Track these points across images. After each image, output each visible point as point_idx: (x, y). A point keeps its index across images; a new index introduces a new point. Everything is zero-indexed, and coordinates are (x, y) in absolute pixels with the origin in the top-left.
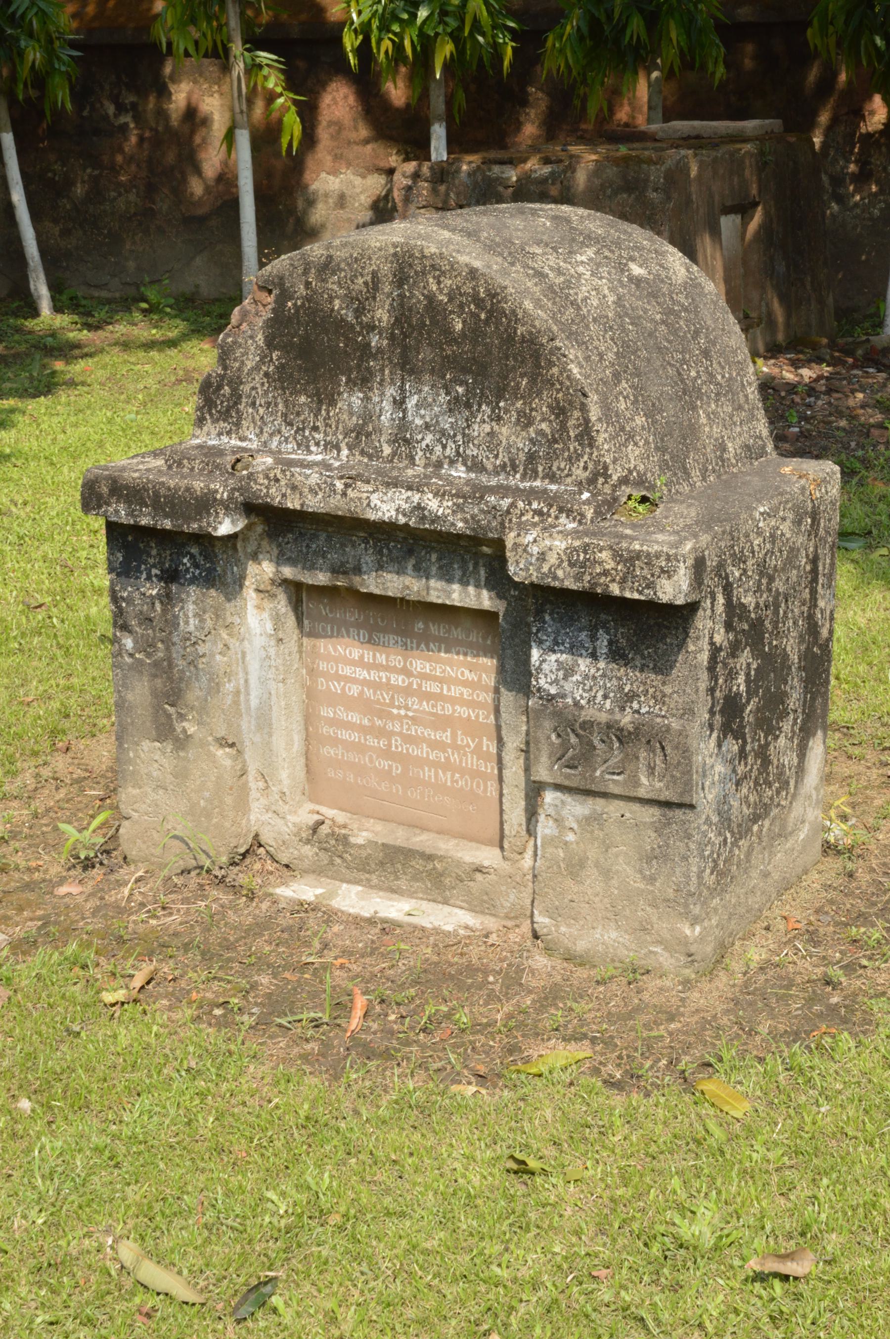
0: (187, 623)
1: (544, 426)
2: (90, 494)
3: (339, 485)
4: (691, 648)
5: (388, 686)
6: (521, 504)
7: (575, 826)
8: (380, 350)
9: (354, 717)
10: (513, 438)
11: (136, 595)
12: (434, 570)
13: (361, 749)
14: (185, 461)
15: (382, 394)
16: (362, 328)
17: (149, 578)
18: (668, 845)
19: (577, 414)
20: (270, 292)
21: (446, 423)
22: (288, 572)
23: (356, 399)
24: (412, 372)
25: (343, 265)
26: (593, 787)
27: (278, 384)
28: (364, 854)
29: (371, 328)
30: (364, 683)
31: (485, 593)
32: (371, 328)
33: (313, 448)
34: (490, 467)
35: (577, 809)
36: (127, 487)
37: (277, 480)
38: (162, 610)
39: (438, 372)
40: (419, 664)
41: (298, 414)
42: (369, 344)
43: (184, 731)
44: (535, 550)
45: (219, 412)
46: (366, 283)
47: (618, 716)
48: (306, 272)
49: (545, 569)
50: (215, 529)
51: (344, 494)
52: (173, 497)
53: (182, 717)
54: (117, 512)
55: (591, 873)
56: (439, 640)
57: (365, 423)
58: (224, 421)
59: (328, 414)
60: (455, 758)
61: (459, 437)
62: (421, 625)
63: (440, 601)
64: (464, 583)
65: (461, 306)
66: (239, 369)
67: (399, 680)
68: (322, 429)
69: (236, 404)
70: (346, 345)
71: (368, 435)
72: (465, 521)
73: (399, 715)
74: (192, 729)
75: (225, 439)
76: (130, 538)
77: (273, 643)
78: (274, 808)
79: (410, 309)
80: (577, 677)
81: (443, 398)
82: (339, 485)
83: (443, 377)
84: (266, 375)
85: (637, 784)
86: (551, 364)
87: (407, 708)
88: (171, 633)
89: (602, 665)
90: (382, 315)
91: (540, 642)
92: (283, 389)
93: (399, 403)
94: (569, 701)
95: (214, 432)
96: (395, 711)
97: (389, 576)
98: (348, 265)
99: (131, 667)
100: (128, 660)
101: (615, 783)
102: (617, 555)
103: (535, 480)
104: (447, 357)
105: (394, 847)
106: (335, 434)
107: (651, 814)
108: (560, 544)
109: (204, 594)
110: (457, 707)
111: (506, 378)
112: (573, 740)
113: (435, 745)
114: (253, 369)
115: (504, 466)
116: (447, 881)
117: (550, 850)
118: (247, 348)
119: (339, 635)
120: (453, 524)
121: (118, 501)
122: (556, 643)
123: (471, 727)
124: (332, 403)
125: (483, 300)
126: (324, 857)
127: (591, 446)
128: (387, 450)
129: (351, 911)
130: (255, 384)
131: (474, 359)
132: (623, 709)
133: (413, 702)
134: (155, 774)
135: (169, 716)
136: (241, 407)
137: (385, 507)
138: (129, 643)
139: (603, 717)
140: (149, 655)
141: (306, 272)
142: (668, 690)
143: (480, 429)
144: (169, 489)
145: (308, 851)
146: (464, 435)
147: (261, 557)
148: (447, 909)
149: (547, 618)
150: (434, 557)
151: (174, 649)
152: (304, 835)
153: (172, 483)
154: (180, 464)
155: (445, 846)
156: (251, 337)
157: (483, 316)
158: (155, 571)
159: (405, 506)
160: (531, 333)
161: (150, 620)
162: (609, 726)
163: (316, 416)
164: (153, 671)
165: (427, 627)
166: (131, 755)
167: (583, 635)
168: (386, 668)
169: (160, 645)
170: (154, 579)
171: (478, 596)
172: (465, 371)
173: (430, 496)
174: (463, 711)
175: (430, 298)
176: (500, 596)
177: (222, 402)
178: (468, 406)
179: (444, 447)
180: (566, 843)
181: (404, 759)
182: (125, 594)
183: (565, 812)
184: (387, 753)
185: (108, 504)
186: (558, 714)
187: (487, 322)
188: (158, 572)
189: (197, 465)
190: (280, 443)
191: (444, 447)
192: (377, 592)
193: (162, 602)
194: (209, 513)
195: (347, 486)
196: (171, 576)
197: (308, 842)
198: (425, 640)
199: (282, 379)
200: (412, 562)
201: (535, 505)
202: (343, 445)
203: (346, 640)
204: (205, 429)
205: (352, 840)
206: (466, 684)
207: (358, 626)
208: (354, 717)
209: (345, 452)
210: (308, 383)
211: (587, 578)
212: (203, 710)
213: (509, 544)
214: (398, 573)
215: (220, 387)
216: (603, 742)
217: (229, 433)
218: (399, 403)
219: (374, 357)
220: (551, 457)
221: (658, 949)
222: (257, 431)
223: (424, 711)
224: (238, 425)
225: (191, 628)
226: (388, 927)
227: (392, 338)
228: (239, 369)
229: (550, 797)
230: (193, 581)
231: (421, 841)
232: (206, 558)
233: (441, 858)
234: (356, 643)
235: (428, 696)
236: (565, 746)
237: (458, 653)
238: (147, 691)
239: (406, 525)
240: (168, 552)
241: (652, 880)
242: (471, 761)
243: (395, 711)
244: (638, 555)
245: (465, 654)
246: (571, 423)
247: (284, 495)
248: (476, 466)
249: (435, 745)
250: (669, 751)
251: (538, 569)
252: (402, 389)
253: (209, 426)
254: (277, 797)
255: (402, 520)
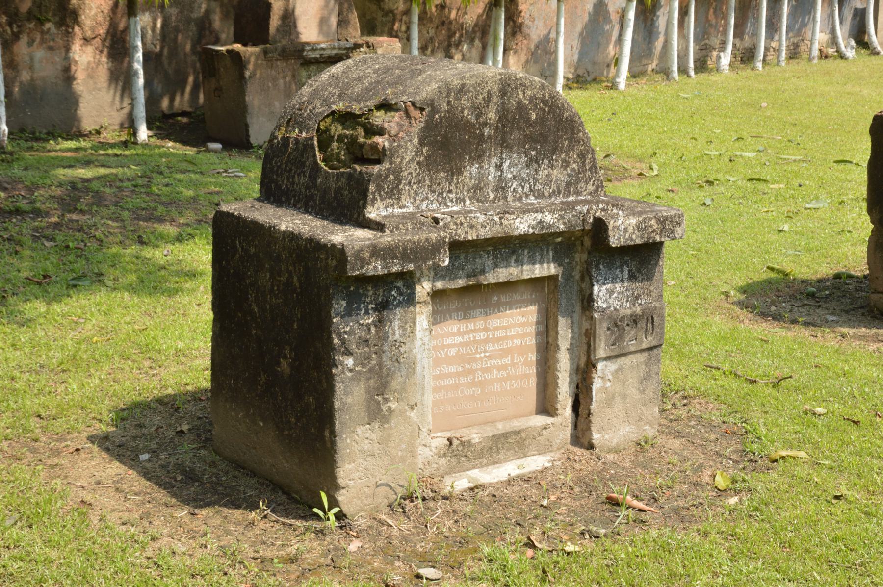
0: (394, 334)
1: (575, 166)
2: (355, 260)
3: (496, 218)
4: (661, 263)
5: (475, 341)
6: (594, 207)
7: (610, 377)
8: (489, 137)
9: (453, 369)
10: (559, 175)
11: (356, 326)
12: (526, 259)
13: (456, 387)
14: (401, 225)
15: (489, 162)
16: (480, 125)
17: (367, 313)
18: (650, 370)
19: (590, 156)
20: (422, 110)
21: (525, 173)
22: (439, 285)
23: (474, 169)
24: (507, 147)
25: (471, 89)
26: (624, 352)
27: (426, 168)
28: (481, 446)
29: (485, 124)
30: (461, 344)
31: (552, 265)
32: (485, 124)
33: (449, 204)
34: (547, 194)
35: (612, 366)
36: (383, 249)
37: (462, 224)
38: (376, 331)
39: (521, 145)
40: (495, 321)
41: (439, 184)
42: (483, 135)
43: (390, 408)
44: (623, 227)
45: (386, 193)
46: (484, 98)
47: (634, 309)
48: (448, 95)
49: (627, 237)
50: (444, 261)
51: (502, 223)
52: (417, 247)
53: (386, 400)
54: (375, 267)
55: (618, 399)
56: (506, 304)
57: (479, 183)
58: (390, 197)
59: (457, 179)
60: (512, 371)
61: (531, 181)
62: (496, 298)
63: (528, 277)
64: (541, 263)
65: (535, 105)
66: (401, 163)
67: (481, 336)
68: (454, 191)
69: (398, 185)
70: (470, 137)
71: (481, 189)
72: (564, 223)
73: (481, 358)
74: (394, 405)
75: (390, 210)
76: (352, 289)
77: (427, 333)
78: (423, 442)
79: (508, 111)
80: (615, 295)
81: (524, 159)
82: (496, 218)
83: (524, 147)
84: (418, 163)
85: (642, 342)
86: (579, 131)
87: (485, 351)
88: (382, 345)
89: (626, 284)
90: (492, 115)
91: (598, 281)
92: (429, 170)
93: (499, 167)
94: (612, 309)
95: (382, 207)
96: (478, 356)
97: (501, 270)
98: (474, 88)
99: (351, 379)
100: (349, 374)
101: (632, 346)
102: (658, 221)
103: (568, 196)
104: (527, 135)
105: (499, 435)
106: (462, 192)
107: (642, 357)
108: (633, 221)
109: (405, 312)
110: (515, 341)
111: (557, 142)
112: (616, 329)
113: (500, 368)
114: (409, 161)
115: (554, 192)
116: (527, 443)
117: (599, 395)
118: (407, 148)
119: (445, 319)
120: (558, 227)
121: (377, 260)
122: (606, 279)
123: (522, 350)
124: (460, 173)
125: (547, 101)
126: (453, 460)
127: (596, 172)
128: (492, 196)
129: (496, 480)
130: (411, 171)
131: (541, 134)
132: (634, 305)
133: (490, 347)
134: (366, 448)
135: (378, 403)
136: (401, 187)
137: (522, 226)
138: (350, 362)
139: (629, 312)
140: (363, 365)
141: (448, 95)
142: (652, 288)
143: (543, 174)
144: (414, 243)
145: (443, 461)
146: (534, 178)
147: (422, 279)
148: (527, 458)
149: (601, 267)
150: (526, 251)
151: (384, 356)
152: (442, 452)
153: (416, 238)
154: (398, 228)
155: (516, 424)
156: (410, 141)
157: (547, 109)
158: (370, 306)
159: (534, 223)
160: (570, 115)
161: (367, 341)
162: (632, 315)
163: (450, 184)
164: (368, 375)
165: (499, 298)
166: (348, 441)
167: (618, 271)
168: (474, 331)
169: (374, 356)
170: (371, 312)
171: (549, 268)
172: (536, 142)
173: (547, 213)
174: (518, 342)
175: (519, 103)
176: (559, 265)
177: (388, 188)
178: (537, 161)
179: (523, 188)
180: (606, 389)
181: (482, 384)
182: (348, 329)
183: (607, 372)
184: (473, 384)
185: (368, 264)
186: (610, 317)
187: (549, 113)
188: (374, 306)
189: (409, 226)
190: (428, 204)
191: (523, 188)
192: (494, 281)
193: (376, 326)
194: (440, 253)
195: (501, 218)
196: (383, 306)
197: (445, 455)
198: (498, 307)
199: (429, 164)
200: (514, 258)
201: (601, 206)
202: (467, 199)
203: (450, 321)
204: (376, 206)
205: (473, 442)
206: (520, 325)
207: (457, 310)
208: (453, 369)
209: (468, 202)
210: (445, 164)
211: (646, 236)
212: (404, 389)
213: (610, 228)
214: (506, 267)
215: (387, 176)
216: (628, 325)
217: (392, 205)
218: (499, 167)
219: (486, 142)
220: (578, 181)
221: (647, 427)
222: (412, 200)
223: (496, 350)
224: (399, 199)
225: (397, 337)
226: (526, 479)
227: (497, 128)
228: (401, 163)
229: (600, 366)
230: (397, 306)
231: (501, 427)
232: (408, 288)
233: (523, 430)
234: (456, 321)
235: (499, 339)
236: (611, 334)
237: (516, 309)
238: (363, 391)
239: (534, 233)
240: (381, 290)
241: (644, 390)
242: (522, 370)
243: (478, 356)
244: (666, 218)
245: (520, 308)
246: (588, 161)
247: (466, 233)
248: (540, 195)
249: (500, 368)
250: (655, 319)
251: (624, 238)
252: (501, 159)
253: (379, 204)
254: (426, 434)
255: (531, 231)
